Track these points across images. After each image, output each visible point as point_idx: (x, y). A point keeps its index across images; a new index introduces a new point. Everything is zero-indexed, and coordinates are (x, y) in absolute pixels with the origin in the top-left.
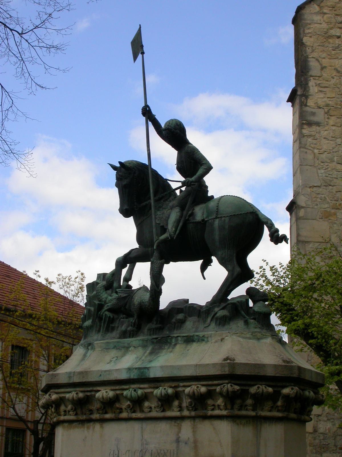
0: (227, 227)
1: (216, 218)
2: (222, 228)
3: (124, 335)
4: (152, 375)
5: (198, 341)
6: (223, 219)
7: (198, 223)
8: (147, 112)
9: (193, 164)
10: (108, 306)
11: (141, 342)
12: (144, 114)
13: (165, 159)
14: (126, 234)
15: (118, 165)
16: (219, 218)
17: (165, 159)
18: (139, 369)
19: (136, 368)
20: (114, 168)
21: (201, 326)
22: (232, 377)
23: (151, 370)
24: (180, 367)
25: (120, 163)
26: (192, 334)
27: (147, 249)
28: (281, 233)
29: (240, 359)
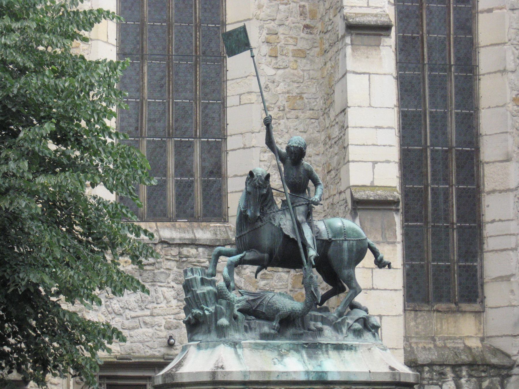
0: (355, 250)
1: (345, 240)
2: (350, 250)
3: (264, 336)
4: (330, 378)
5: (347, 349)
6: (351, 242)
10: (238, 306)
11: (291, 346)
16: (347, 240)
18: (317, 372)
19: (314, 372)
21: (340, 337)
23: (329, 374)
24: (355, 373)
26: (340, 343)
27: (263, 254)
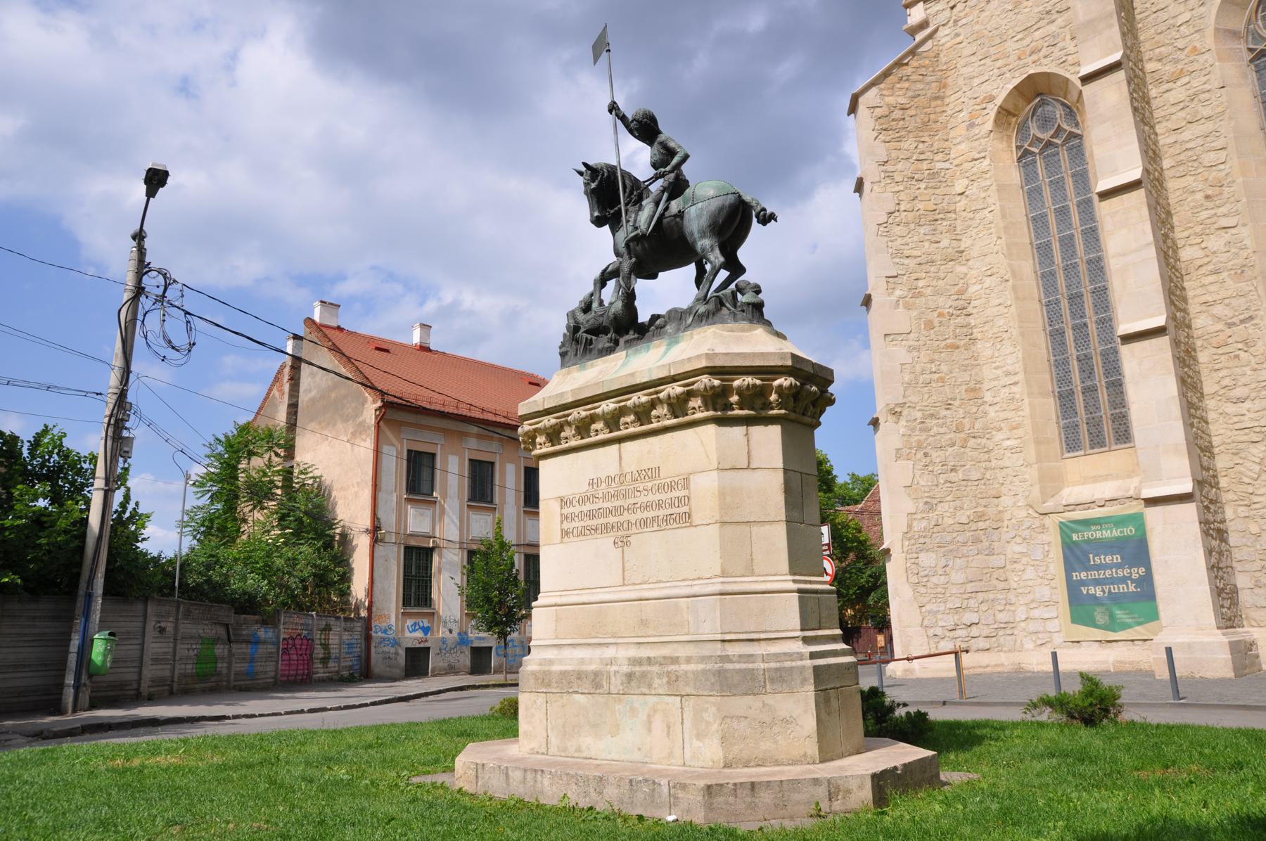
7: (675, 216)
8: (613, 108)
9: (666, 157)
12: (610, 111)
13: (636, 159)
14: (602, 247)
15: (583, 169)
17: (636, 159)
20: (581, 173)
22: (713, 371)
25: (585, 164)
28: (768, 212)
29: (721, 349)
